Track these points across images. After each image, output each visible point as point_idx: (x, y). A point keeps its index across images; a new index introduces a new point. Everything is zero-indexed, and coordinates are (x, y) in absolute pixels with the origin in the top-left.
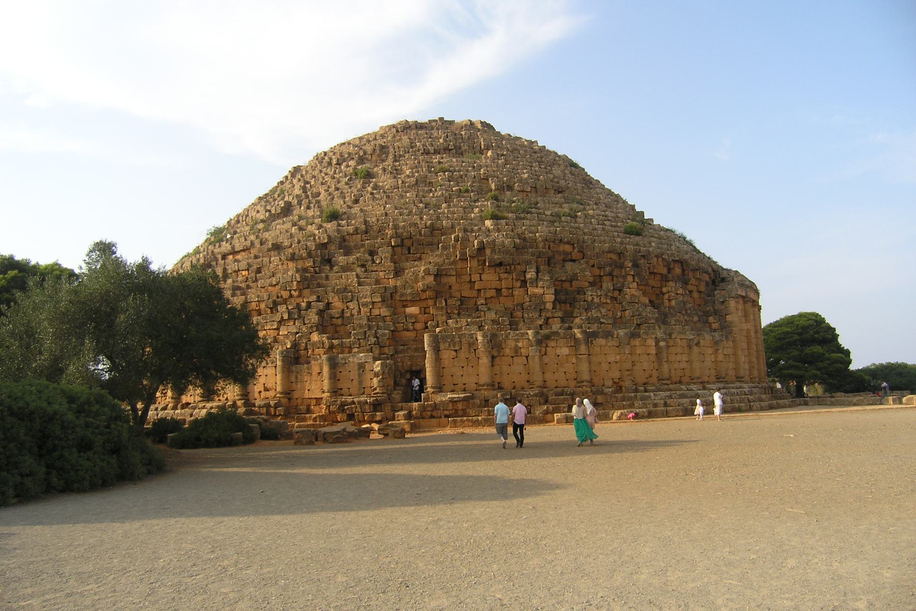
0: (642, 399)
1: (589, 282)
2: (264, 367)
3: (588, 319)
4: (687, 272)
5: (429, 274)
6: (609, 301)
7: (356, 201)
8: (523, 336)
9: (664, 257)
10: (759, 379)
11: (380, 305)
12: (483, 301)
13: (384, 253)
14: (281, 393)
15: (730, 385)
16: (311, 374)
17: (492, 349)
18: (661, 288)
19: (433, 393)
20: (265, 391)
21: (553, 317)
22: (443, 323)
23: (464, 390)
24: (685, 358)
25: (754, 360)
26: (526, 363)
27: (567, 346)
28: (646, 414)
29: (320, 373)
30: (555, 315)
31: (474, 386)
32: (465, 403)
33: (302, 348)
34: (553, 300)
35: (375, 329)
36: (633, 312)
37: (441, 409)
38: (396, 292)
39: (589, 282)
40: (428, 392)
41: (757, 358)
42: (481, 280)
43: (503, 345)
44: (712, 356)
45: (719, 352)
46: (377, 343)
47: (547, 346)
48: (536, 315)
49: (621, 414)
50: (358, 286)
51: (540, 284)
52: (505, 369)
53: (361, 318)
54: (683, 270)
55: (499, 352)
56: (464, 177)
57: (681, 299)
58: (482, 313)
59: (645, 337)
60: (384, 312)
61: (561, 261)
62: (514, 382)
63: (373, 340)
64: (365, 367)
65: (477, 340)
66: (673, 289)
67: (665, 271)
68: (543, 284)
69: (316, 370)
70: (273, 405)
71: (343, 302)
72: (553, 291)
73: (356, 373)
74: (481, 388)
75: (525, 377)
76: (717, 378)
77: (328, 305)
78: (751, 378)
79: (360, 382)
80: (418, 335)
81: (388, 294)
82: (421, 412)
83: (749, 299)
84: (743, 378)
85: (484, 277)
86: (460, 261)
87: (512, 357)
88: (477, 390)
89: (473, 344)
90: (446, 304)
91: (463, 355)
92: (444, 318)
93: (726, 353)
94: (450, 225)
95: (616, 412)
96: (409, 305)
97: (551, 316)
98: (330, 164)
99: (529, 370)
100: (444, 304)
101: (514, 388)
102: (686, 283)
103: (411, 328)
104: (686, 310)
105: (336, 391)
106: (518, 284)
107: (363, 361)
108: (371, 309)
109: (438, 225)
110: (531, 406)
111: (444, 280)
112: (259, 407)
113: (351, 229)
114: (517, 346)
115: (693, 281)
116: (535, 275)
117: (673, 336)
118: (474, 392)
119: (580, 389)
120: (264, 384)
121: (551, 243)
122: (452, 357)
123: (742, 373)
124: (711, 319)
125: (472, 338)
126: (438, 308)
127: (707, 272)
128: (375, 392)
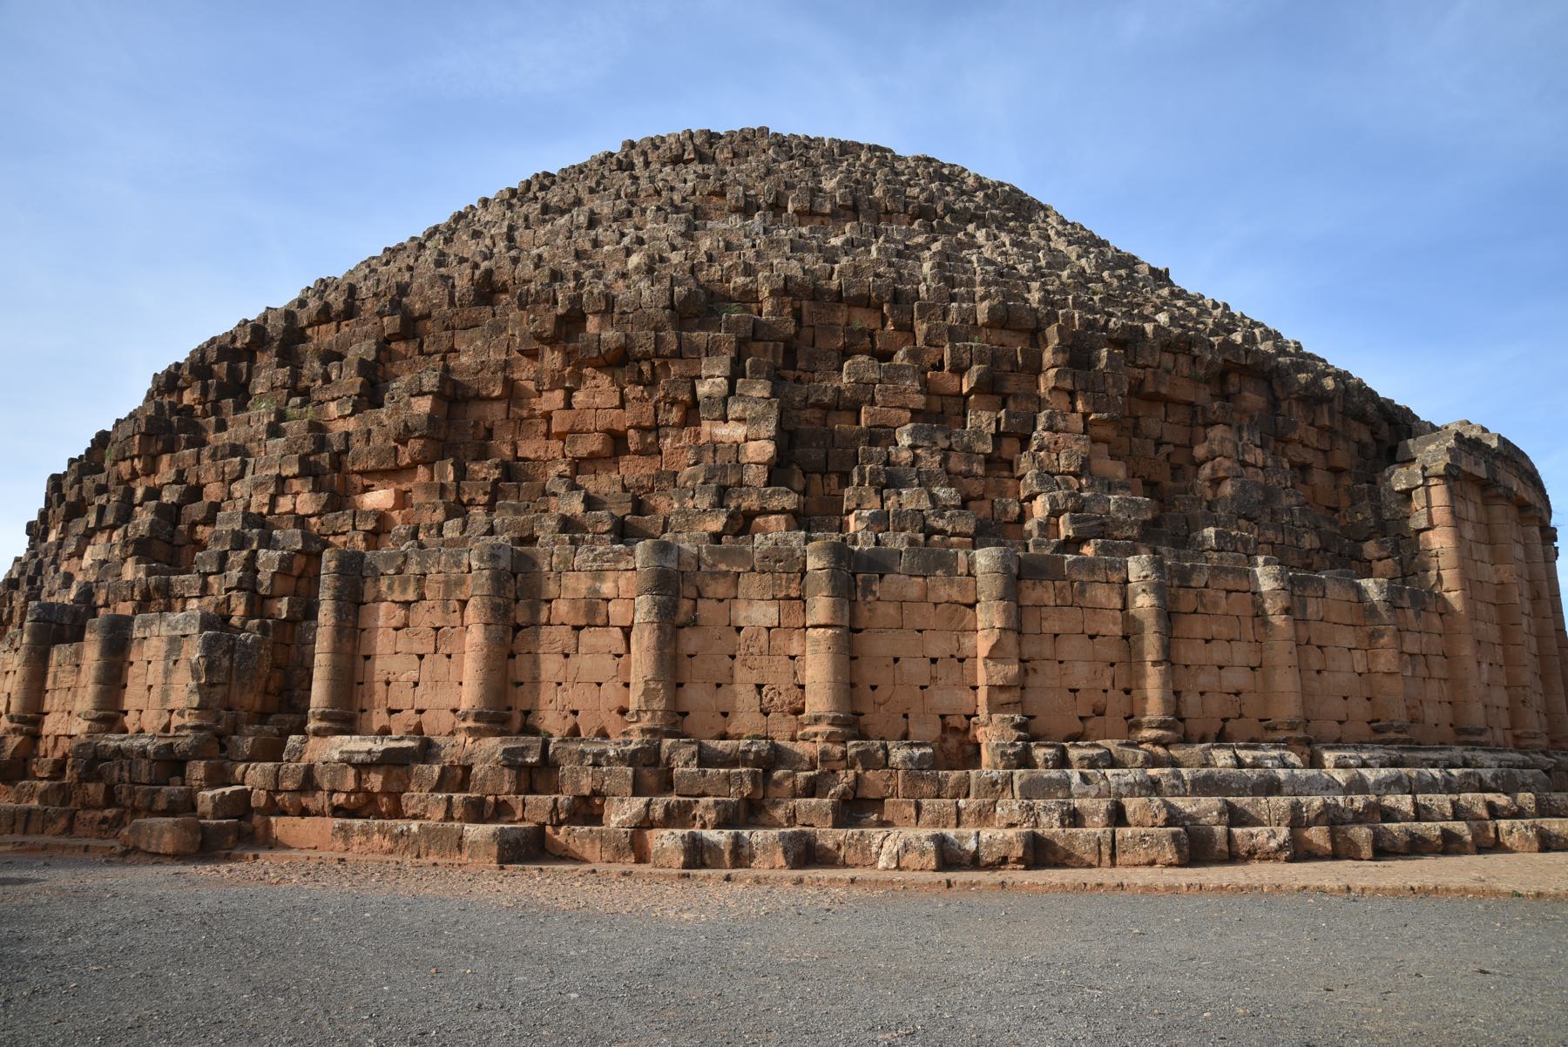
1: (913, 411)
4: (1285, 405)
5: (421, 394)
8: (618, 562)
9: (1196, 351)
10: (1553, 741)
11: (296, 485)
15: (1423, 755)
17: (517, 600)
18: (1191, 447)
19: (317, 733)
21: (764, 512)
22: (431, 527)
24: (1242, 654)
25: (1527, 676)
26: (622, 650)
27: (774, 598)
28: (1018, 851)
30: (775, 503)
31: (447, 720)
32: (396, 771)
35: (255, 546)
37: (326, 786)
41: (1543, 677)
42: (568, 405)
43: (551, 589)
44: (1357, 654)
45: (1384, 640)
47: (700, 596)
48: (704, 502)
49: (906, 847)
50: (268, 438)
51: (735, 409)
52: (550, 666)
54: (1274, 403)
55: (535, 612)
57: (1261, 479)
60: (305, 501)
62: (575, 713)
66: (1229, 447)
68: (744, 410)
71: (223, 481)
72: (769, 428)
75: (611, 694)
76: (1376, 731)
77: (195, 493)
78: (1517, 737)
79: (165, 697)
83: (1501, 491)
84: (1481, 732)
85: (579, 397)
87: (577, 628)
89: (460, 583)
90: (458, 479)
91: (424, 617)
92: (439, 515)
93: (1416, 650)
97: (756, 507)
99: (628, 673)
100: (451, 477)
104: (1273, 512)
106: (675, 415)
107: (179, 633)
110: (603, 796)
111: (475, 412)
114: (597, 591)
115: (1303, 431)
117: (1198, 580)
119: (807, 744)
121: (805, 303)
122: (394, 623)
123: (1476, 715)
124: (1370, 549)
125: (458, 564)
127: (1361, 417)
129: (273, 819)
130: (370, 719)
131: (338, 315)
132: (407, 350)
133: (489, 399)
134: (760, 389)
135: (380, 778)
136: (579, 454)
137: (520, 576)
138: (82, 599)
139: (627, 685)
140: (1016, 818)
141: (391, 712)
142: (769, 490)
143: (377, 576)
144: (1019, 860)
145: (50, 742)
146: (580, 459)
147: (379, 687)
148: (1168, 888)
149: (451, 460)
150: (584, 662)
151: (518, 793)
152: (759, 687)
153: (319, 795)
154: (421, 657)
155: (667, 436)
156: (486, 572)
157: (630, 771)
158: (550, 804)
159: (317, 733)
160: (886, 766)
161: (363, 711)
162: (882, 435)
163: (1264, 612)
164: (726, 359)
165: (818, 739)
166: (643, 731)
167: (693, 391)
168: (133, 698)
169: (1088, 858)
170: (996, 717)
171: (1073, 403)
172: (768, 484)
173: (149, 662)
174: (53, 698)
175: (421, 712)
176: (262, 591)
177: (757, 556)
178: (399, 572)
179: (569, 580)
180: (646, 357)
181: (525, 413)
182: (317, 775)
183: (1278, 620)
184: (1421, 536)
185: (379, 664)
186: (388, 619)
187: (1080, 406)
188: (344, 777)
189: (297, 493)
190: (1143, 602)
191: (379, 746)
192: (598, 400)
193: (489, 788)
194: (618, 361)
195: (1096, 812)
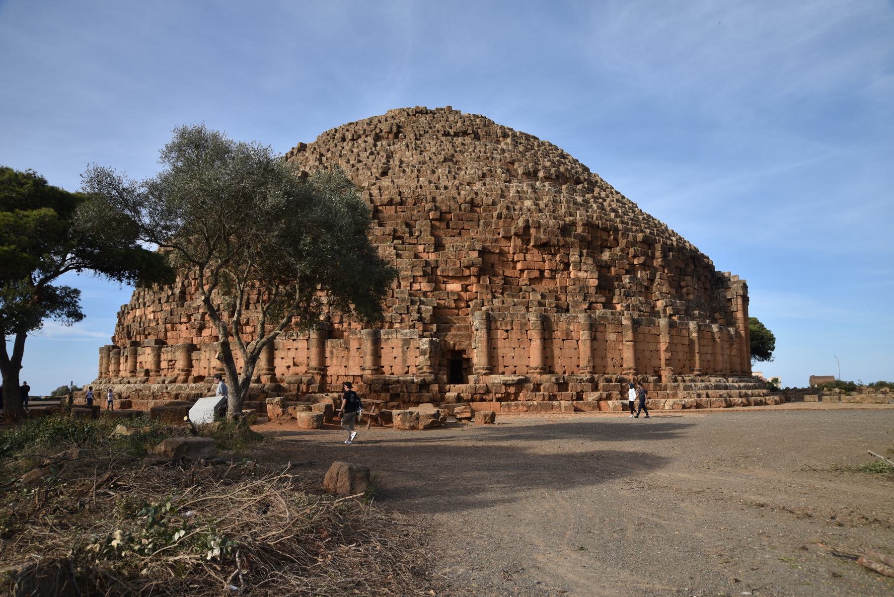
0: (686, 388)
1: (625, 270)
2: (294, 340)
3: (627, 308)
5: (474, 250)
6: (643, 290)
7: (384, 174)
11: (420, 279)
12: (527, 282)
13: (422, 226)
14: (315, 369)
16: (349, 351)
18: (680, 282)
19: (485, 374)
20: (294, 365)
21: (596, 303)
23: (515, 373)
26: (577, 347)
28: (695, 404)
29: (359, 348)
32: (518, 386)
33: (336, 322)
34: (596, 285)
35: (418, 304)
36: (666, 302)
37: (494, 392)
38: (437, 267)
39: (625, 270)
40: (479, 373)
43: (555, 327)
45: (734, 346)
46: (421, 319)
47: (596, 331)
48: (580, 298)
51: (584, 267)
52: (557, 352)
53: (402, 292)
55: (551, 335)
56: (490, 159)
58: (527, 294)
59: (680, 327)
60: (425, 286)
61: (599, 247)
62: (564, 367)
63: (416, 316)
64: (410, 344)
65: (529, 320)
67: (683, 266)
68: (587, 268)
69: (354, 345)
70: (306, 382)
72: (596, 275)
73: (400, 350)
74: (532, 371)
75: (574, 361)
79: (404, 361)
80: (460, 313)
81: (429, 270)
82: (473, 395)
85: (528, 256)
86: (503, 239)
87: (563, 340)
88: (527, 373)
89: (526, 324)
91: (514, 335)
92: (490, 296)
94: (490, 202)
95: (668, 400)
96: (450, 281)
98: (343, 139)
100: (488, 282)
101: (564, 373)
102: (698, 280)
103: (453, 305)
105: (378, 368)
106: (562, 267)
108: (411, 283)
109: (477, 201)
111: (487, 257)
112: (289, 383)
113: (385, 198)
114: (568, 329)
116: (579, 259)
118: (527, 375)
120: (294, 358)
121: (590, 229)
122: (503, 337)
125: (524, 318)
126: (482, 286)
128: (421, 371)
129: (471, 403)
130: (498, 369)
131: (396, 204)
132: (440, 225)
133: (494, 253)
134: (590, 261)
135: (514, 388)
136: (531, 277)
137: (545, 323)
138: (327, 320)
139: (579, 358)
140: (686, 396)
141: (505, 367)
142: (597, 295)
143: (496, 321)
144: (695, 406)
145: (334, 378)
146: (532, 279)
147: (500, 359)
148: (748, 410)
149: (488, 276)
150: (566, 351)
151: (559, 391)
152: (613, 359)
153: (491, 395)
154: (514, 348)
155: (559, 273)
156: (539, 322)
157: (590, 384)
158: (571, 395)
159: (485, 374)
160: (647, 382)
161: (494, 366)
162: (618, 278)
163: (714, 338)
164: (578, 249)
165: (631, 374)
166: (589, 372)
167: (569, 259)
168: (385, 361)
169: (705, 406)
170: (667, 368)
171: (664, 270)
172: (596, 293)
173: (393, 348)
174: (332, 360)
175: (515, 367)
176: (426, 321)
177: (610, 319)
178: (503, 319)
179: (560, 324)
180: (554, 246)
181: (506, 259)
182: (490, 388)
183: (718, 340)
184: (734, 313)
185: (499, 351)
186: (501, 336)
187: (666, 271)
188: (501, 388)
189: (420, 283)
190: (695, 335)
191: (516, 378)
192: (535, 258)
193: (550, 390)
194: (543, 246)
195: (703, 394)
